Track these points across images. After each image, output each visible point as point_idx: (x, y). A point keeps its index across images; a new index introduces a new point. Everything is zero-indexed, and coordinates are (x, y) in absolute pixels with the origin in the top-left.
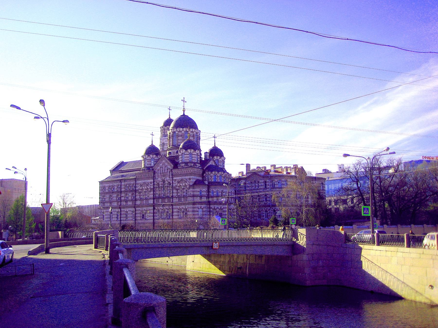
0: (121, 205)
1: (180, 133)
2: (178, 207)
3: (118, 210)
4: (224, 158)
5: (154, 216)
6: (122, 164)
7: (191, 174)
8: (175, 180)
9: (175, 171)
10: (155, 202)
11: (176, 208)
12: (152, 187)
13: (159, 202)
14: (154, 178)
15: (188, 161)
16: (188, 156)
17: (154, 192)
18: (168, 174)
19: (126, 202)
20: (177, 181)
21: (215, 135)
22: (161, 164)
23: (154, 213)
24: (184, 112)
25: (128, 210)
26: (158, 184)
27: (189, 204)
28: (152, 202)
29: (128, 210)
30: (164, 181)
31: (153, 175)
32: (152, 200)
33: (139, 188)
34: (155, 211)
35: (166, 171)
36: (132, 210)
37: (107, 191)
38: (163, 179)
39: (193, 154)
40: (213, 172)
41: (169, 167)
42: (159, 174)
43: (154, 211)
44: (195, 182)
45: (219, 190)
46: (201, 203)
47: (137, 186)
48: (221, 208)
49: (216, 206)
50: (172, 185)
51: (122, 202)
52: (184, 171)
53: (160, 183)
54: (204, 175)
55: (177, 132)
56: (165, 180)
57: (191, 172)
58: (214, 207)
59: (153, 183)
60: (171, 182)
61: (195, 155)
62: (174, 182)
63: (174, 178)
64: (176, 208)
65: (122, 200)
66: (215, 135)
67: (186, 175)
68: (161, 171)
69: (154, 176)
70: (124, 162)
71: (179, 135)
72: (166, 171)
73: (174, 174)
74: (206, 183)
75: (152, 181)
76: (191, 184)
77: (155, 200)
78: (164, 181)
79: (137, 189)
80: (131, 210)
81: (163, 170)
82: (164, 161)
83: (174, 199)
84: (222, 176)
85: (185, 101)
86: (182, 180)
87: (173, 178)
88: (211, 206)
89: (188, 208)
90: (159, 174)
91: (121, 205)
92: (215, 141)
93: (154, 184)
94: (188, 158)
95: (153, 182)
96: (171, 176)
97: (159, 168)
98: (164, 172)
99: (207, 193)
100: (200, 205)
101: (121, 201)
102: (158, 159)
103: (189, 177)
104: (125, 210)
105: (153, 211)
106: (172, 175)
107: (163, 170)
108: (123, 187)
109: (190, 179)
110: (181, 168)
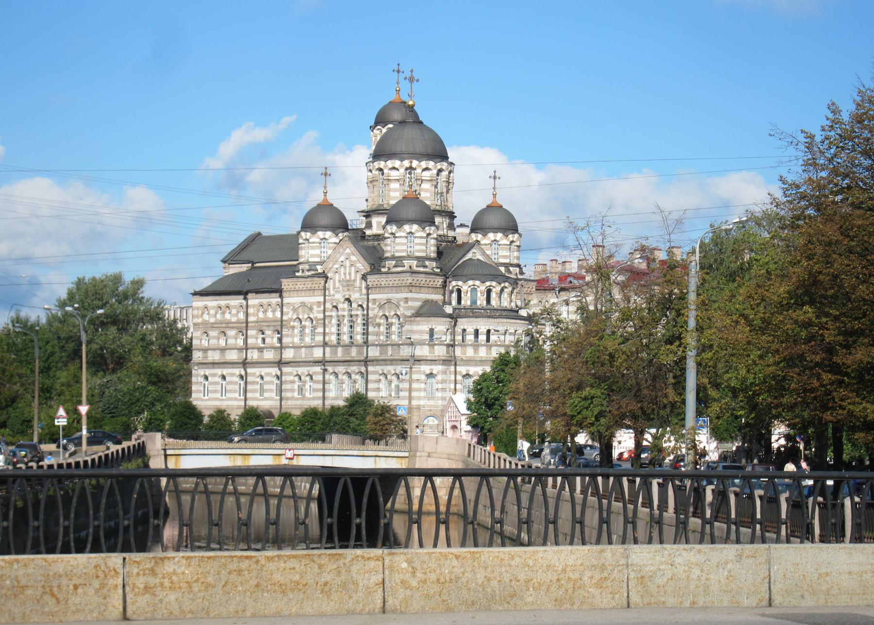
0: (246, 359)
1: (394, 173)
2: (379, 369)
5: (324, 390)
6: (256, 237)
7: (411, 287)
9: (372, 279)
10: (328, 355)
12: (321, 316)
13: (336, 353)
15: (404, 254)
16: (404, 241)
17: (324, 330)
18: (358, 284)
19: (260, 350)
20: (377, 304)
21: (495, 172)
23: (324, 383)
25: (264, 371)
27: (403, 360)
28: (321, 355)
29: (263, 374)
33: (290, 316)
34: (327, 377)
38: (347, 297)
41: (359, 265)
42: (337, 285)
43: (324, 377)
44: (421, 307)
46: (433, 361)
47: (285, 309)
50: (365, 312)
51: (249, 351)
52: (393, 280)
53: (340, 306)
55: (386, 171)
57: (408, 284)
59: (322, 306)
60: (365, 306)
62: (370, 304)
63: (371, 297)
65: (249, 346)
66: (495, 172)
67: (398, 288)
68: (342, 274)
69: (325, 289)
70: (264, 234)
71: (391, 178)
72: (353, 278)
73: (371, 286)
75: (321, 299)
76: (409, 313)
77: (328, 350)
79: (285, 318)
81: (345, 274)
82: (348, 251)
83: (369, 348)
85: (416, 78)
86: (389, 301)
87: (368, 295)
90: (337, 285)
92: (494, 188)
94: (404, 248)
95: (322, 303)
96: (364, 291)
98: (348, 277)
101: (247, 349)
103: (404, 295)
105: (322, 376)
106: (368, 288)
107: (345, 274)
108: (251, 311)
109: (406, 300)
110: (386, 273)
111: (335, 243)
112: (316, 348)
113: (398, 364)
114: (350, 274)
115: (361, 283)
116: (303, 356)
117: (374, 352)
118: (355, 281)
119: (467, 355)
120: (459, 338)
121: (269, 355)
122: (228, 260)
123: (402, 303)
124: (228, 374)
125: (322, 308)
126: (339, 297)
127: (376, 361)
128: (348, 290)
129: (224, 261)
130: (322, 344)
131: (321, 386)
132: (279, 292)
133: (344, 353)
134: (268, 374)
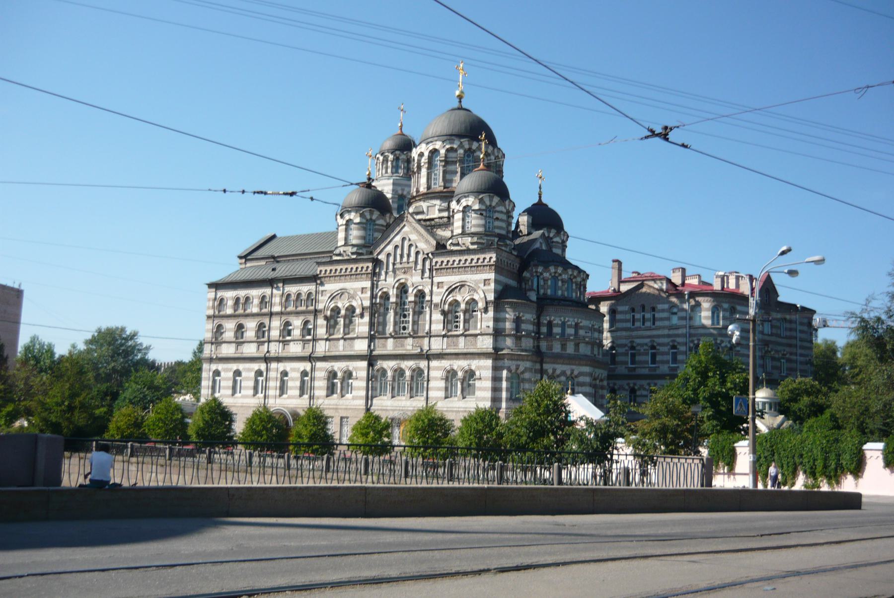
1: (452, 155)
2: (446, 364)
3: (260, 366)
4: (566, 237)
8: (440, 285)
11: (437, 369)
12: (367, 303)
14: (374, 274)
20: (446, 288)
22: (398, 239)
24: (460, 102)
25: (288, 366)
26: (386, 296)
29: (288, 369)
30: (403, 289)
31: (370, 268)
32: (366, 342)
35: (412, 259)
36: (302, 369)
37: (229, 311)
39: (498, 212)
40: (550, 268)
41: (422, 246)
45: (568, 321)
48: (572, 373)
49: (560, 368)
54: (526, 274)
56: (409, 284)
58: (554, 370)
60: (427, 291)
61: (502, 212)
62: (435, 288)
63: (436, 280)
64: (437, 369)
72: (412, 259)
74: (533, 296)
75: (368, 284)
78: (403, 289)
80: (299, 369)
82: (406, 229)
84: (574, 280)
87: (431, 277)
88: (545, 366)
89: (479, 368)
91: (268, 352)
93: (373, 297)
96: (427, 274)
97: (390, 248)
99: (535, 327)
100: (514, 362)
102: (385, 224)
104: (282, 366)
106: (431, 270)
107: (402, 256)
111: (382, 226)
112: (360, 340)
113: (474, 359)
114: (409, 255)
115: (424, 265)
116: (341, 348)
117: (437, 345)
118: (416, 262)
119: (553, 351)
120: (544, 330)
121: (295, 349)
122: (246, 257)
123: (482, 285)
124: (244, 369)
125: (368, 294)
126: (391, 280)
127: (440, 356)
128: (404, 273)
129: (240, 257)
130: (367, 335)
131: (364, 384)
132: (314, 279)
133: (395, 346)
134: (293, 370)
